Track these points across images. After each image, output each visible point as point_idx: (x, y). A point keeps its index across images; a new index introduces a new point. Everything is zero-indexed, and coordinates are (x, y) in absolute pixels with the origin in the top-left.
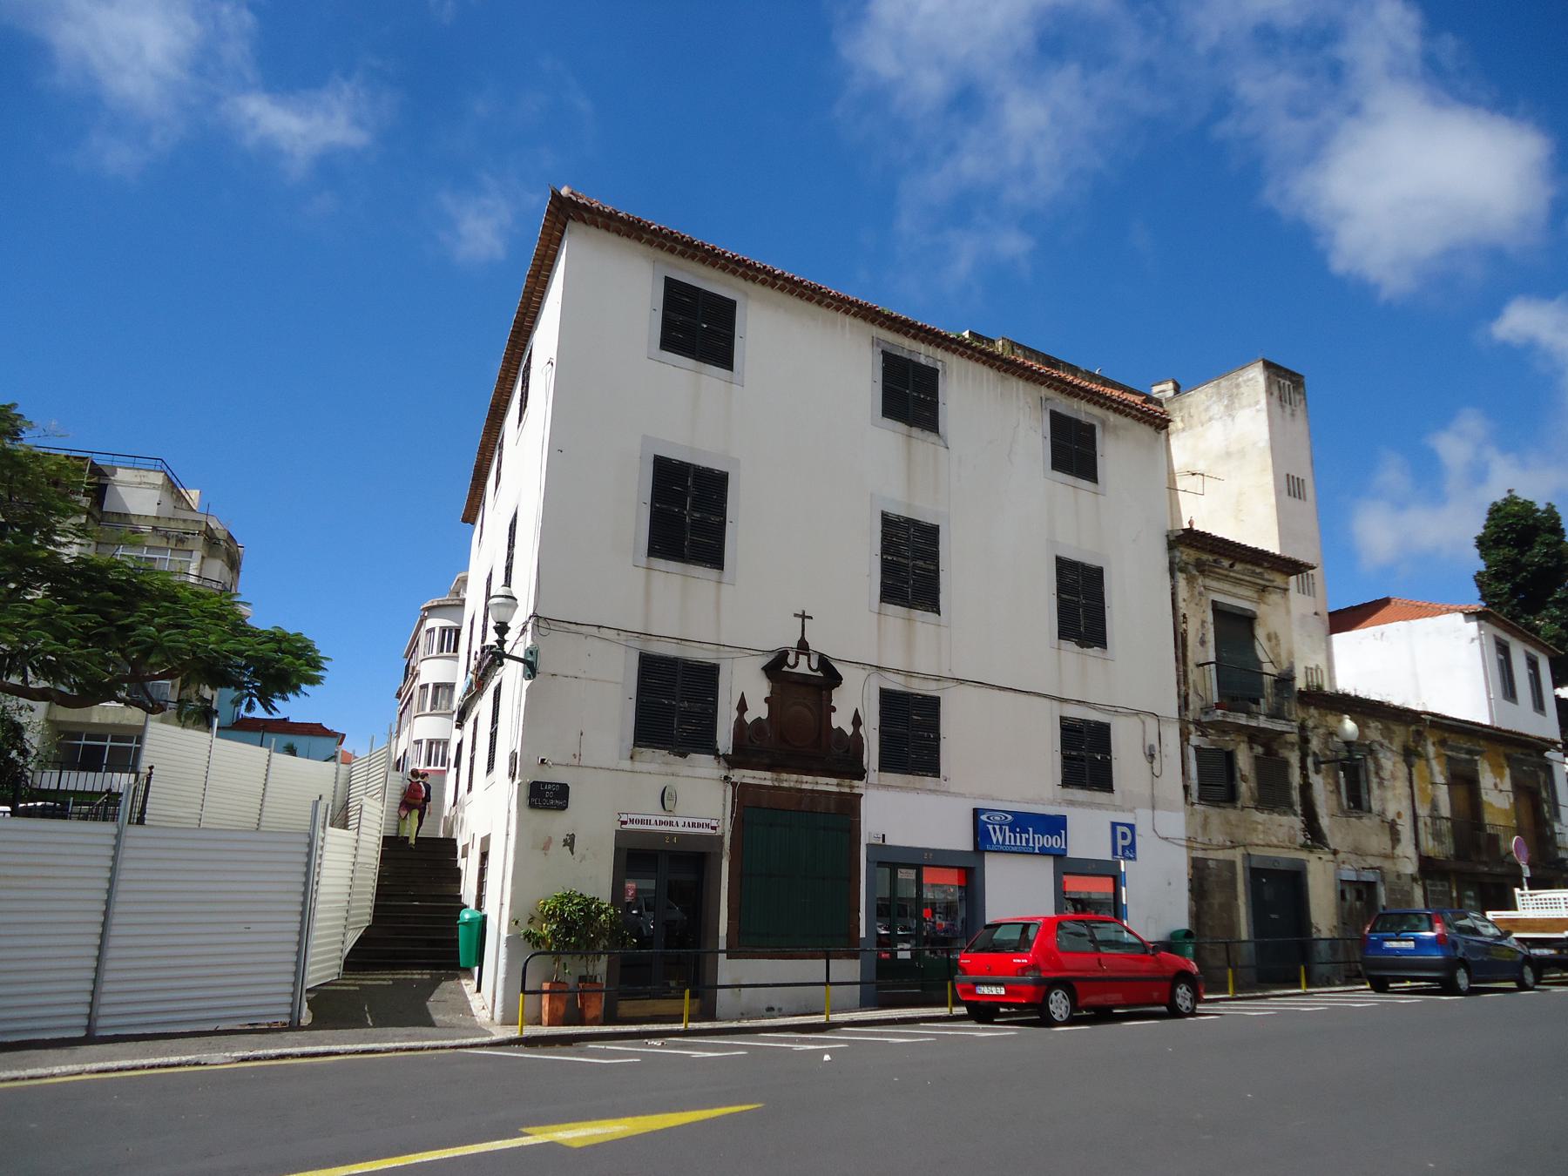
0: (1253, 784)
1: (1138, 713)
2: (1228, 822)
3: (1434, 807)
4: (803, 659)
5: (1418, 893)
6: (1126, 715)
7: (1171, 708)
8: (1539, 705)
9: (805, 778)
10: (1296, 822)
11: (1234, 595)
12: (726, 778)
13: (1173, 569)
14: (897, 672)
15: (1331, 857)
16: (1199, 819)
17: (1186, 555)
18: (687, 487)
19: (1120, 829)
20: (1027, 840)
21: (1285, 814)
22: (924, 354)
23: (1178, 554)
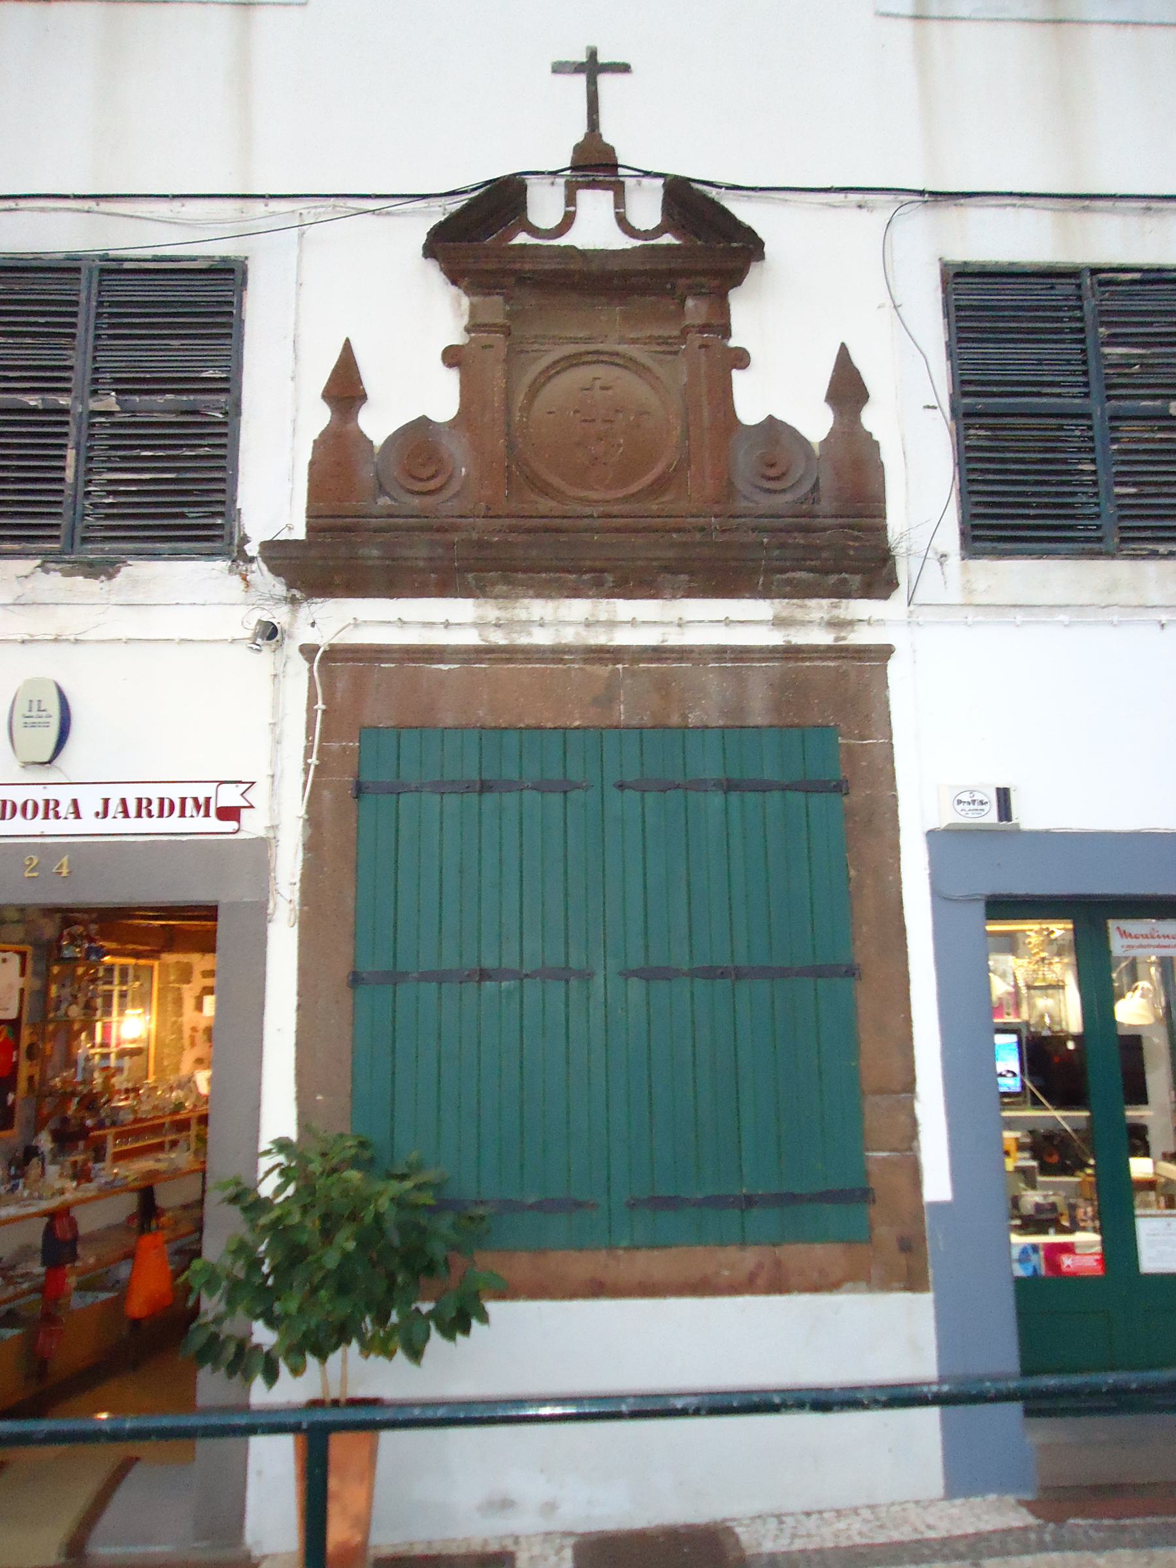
9: (624, 608)
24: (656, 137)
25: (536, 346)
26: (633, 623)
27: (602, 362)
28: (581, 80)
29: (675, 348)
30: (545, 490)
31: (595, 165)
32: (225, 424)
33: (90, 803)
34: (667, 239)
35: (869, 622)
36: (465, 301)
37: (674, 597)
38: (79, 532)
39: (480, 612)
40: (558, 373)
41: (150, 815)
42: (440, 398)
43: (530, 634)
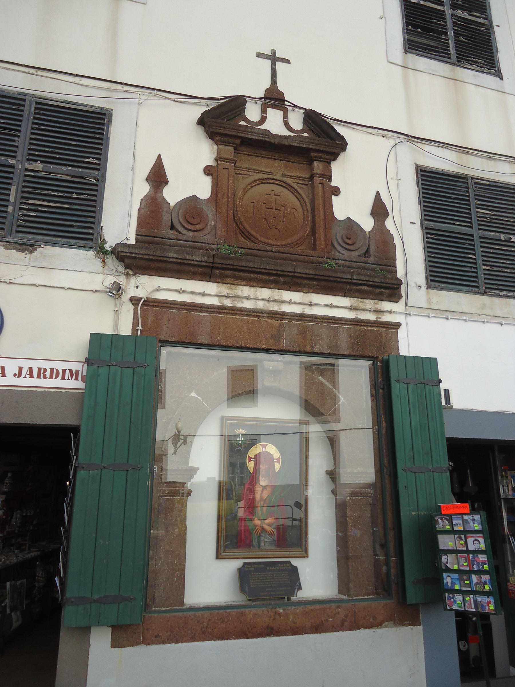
12: (116, 291)
24: (304, 92)
25: (246, 172)
26: (289, 302)
27: (275, 184)
28: (268, 62)
29: (306, 183)
32: (97, 185)
33: (11, 367)
34: (305, 134)
35: (390, 312)
36: (216, 147)
37: (308, 292)
38: (14, 228)
39: (219, 289)
40: (255, 185)
41: (45, 377)
43: (242, 302)
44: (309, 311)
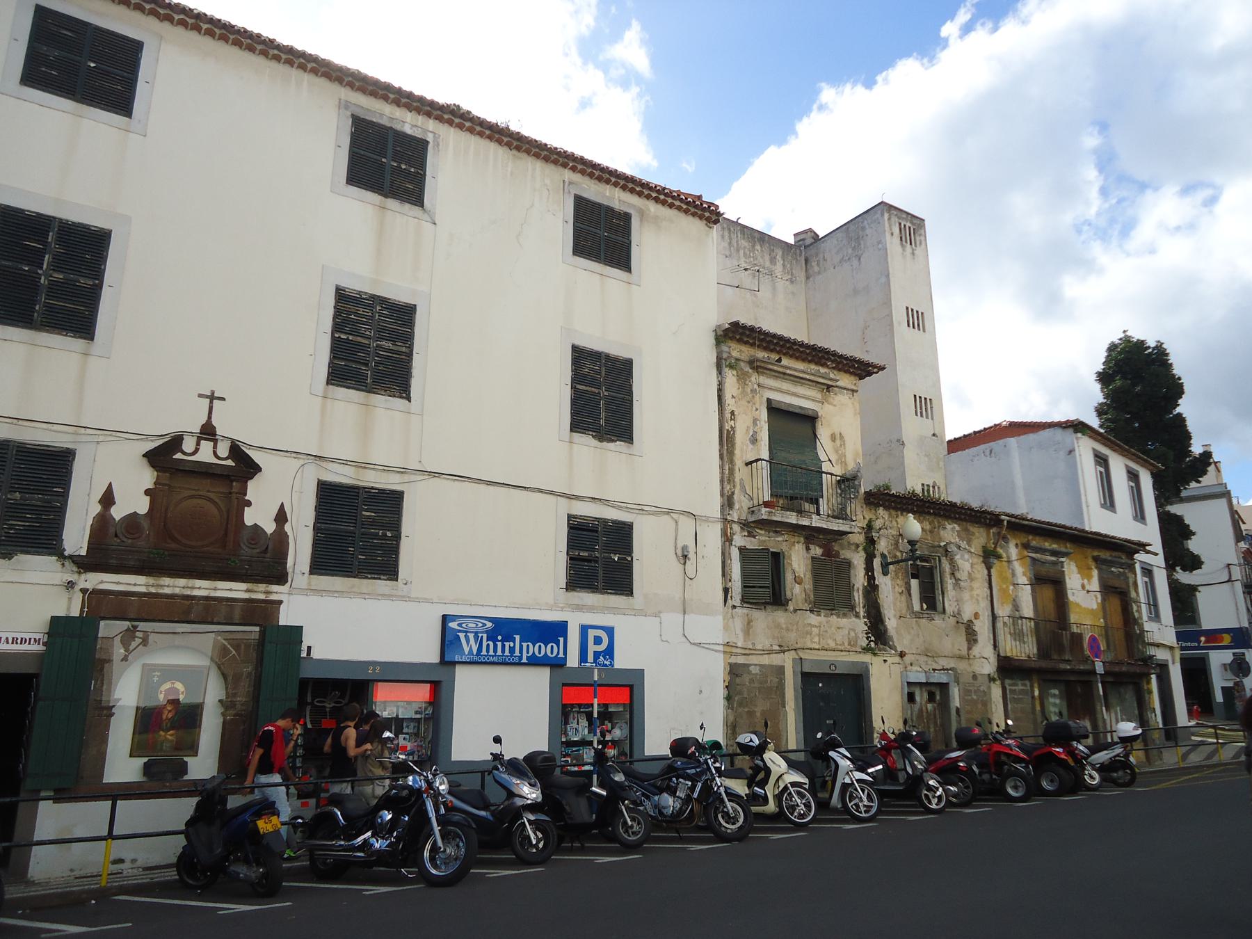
0: (808, 585)
1: (669, 512)
2: (778, 626)
3: (1016, 607)
4: (206, 446)
5: (996, 692)
6: (654, 513)
7: (713, 506)
8: (1140, 516)
9: (198, 583)
10: (859, 625)
11: (794, 394)
12: (70, 585)
13: (720, 364)
14: (346, 462)
15: (897, 659)
16: (738, 624)
17: (737, 351)
18: (45, 243)
19: (592, 634)
20: (512, 650)
21: (845, 615)
22: (410, 123)
23: (725, 348)
30: (174, 539)
31: (208, 432)
42: (142, 506)
44: (213, 594)
